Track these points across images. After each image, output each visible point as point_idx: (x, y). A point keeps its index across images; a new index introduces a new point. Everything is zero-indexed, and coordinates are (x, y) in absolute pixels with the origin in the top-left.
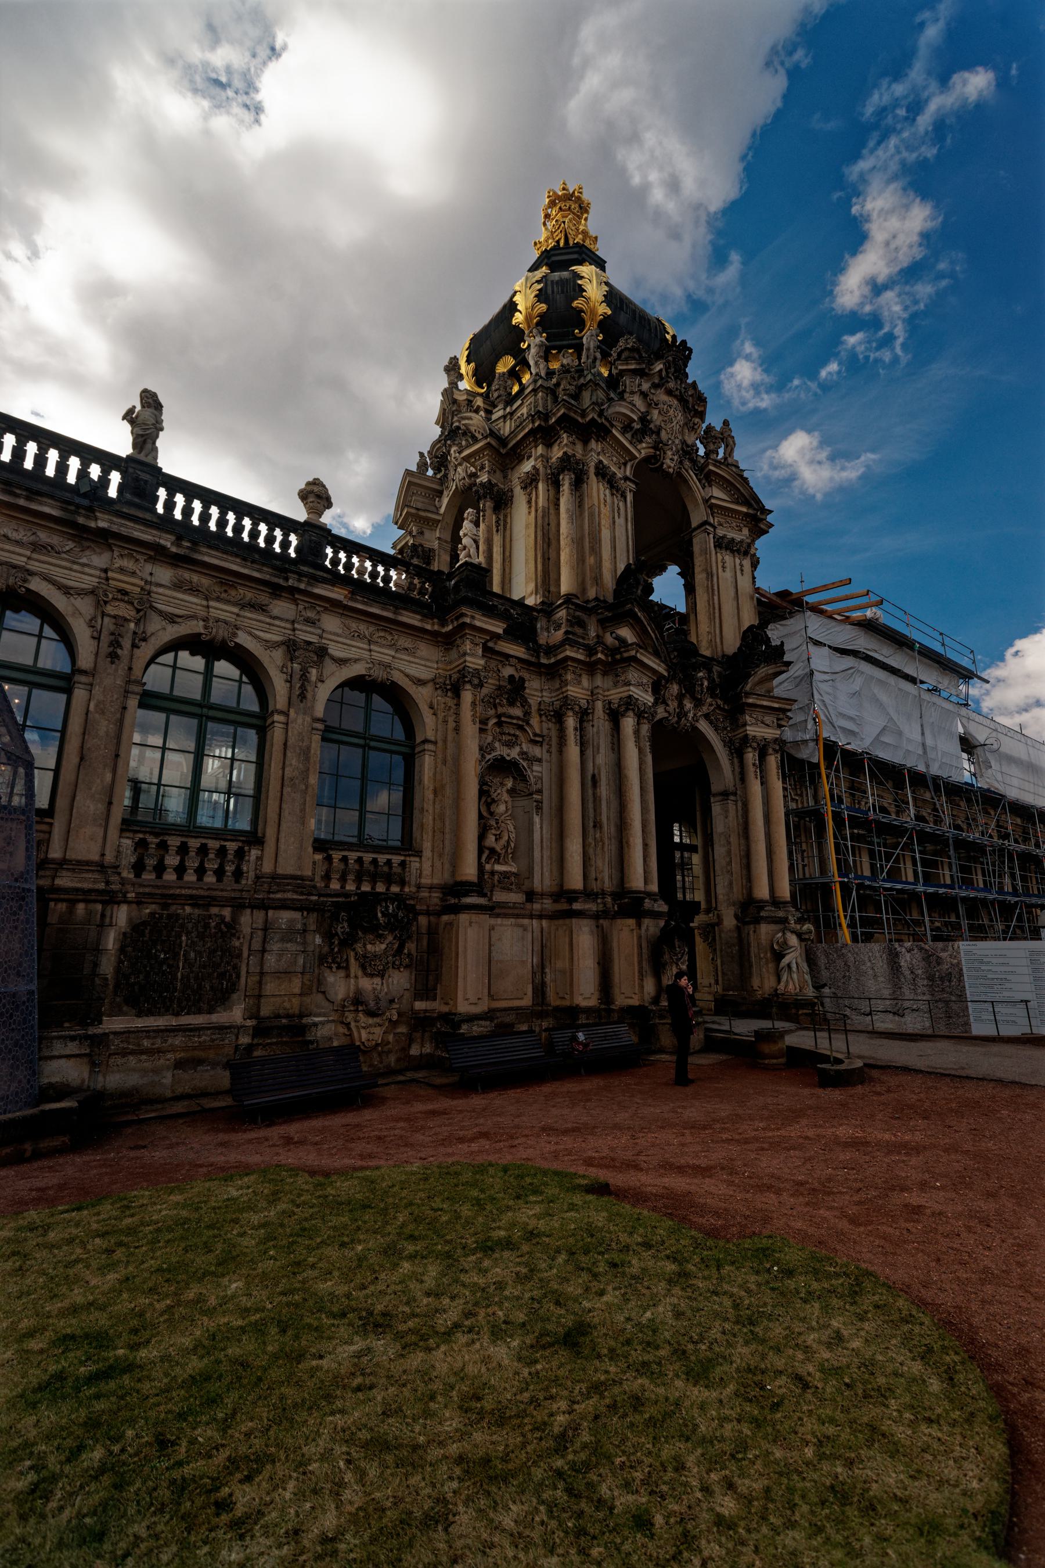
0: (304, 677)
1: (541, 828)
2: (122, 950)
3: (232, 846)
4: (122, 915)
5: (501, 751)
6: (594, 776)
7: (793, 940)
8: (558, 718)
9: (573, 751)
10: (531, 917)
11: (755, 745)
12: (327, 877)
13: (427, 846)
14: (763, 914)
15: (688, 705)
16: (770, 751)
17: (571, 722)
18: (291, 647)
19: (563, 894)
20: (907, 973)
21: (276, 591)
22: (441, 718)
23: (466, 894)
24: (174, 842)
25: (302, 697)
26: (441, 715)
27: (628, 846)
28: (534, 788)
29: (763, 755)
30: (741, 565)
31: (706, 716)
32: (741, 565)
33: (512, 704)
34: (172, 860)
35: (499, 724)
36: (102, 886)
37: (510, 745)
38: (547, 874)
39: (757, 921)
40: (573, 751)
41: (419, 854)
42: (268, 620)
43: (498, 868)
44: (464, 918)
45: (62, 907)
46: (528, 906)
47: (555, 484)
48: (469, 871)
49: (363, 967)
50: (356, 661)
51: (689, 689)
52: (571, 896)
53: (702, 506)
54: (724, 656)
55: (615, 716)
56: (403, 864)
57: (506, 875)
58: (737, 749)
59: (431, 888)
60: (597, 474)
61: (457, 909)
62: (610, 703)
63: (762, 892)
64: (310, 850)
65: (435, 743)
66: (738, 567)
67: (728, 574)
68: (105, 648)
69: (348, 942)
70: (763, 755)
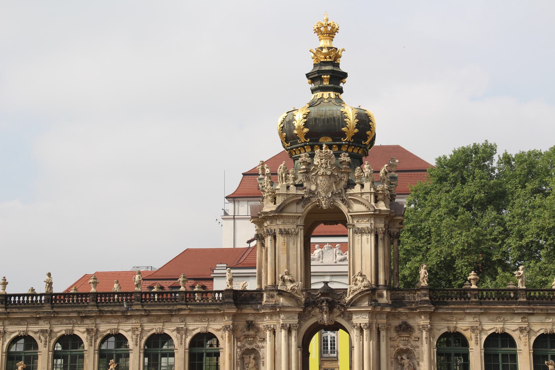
0: (182, 338)
5: (248, 346)
21: (172, 316)
25: (181, 344)
33: (249, 330)
37: (250, 344)
50: (197, 329)
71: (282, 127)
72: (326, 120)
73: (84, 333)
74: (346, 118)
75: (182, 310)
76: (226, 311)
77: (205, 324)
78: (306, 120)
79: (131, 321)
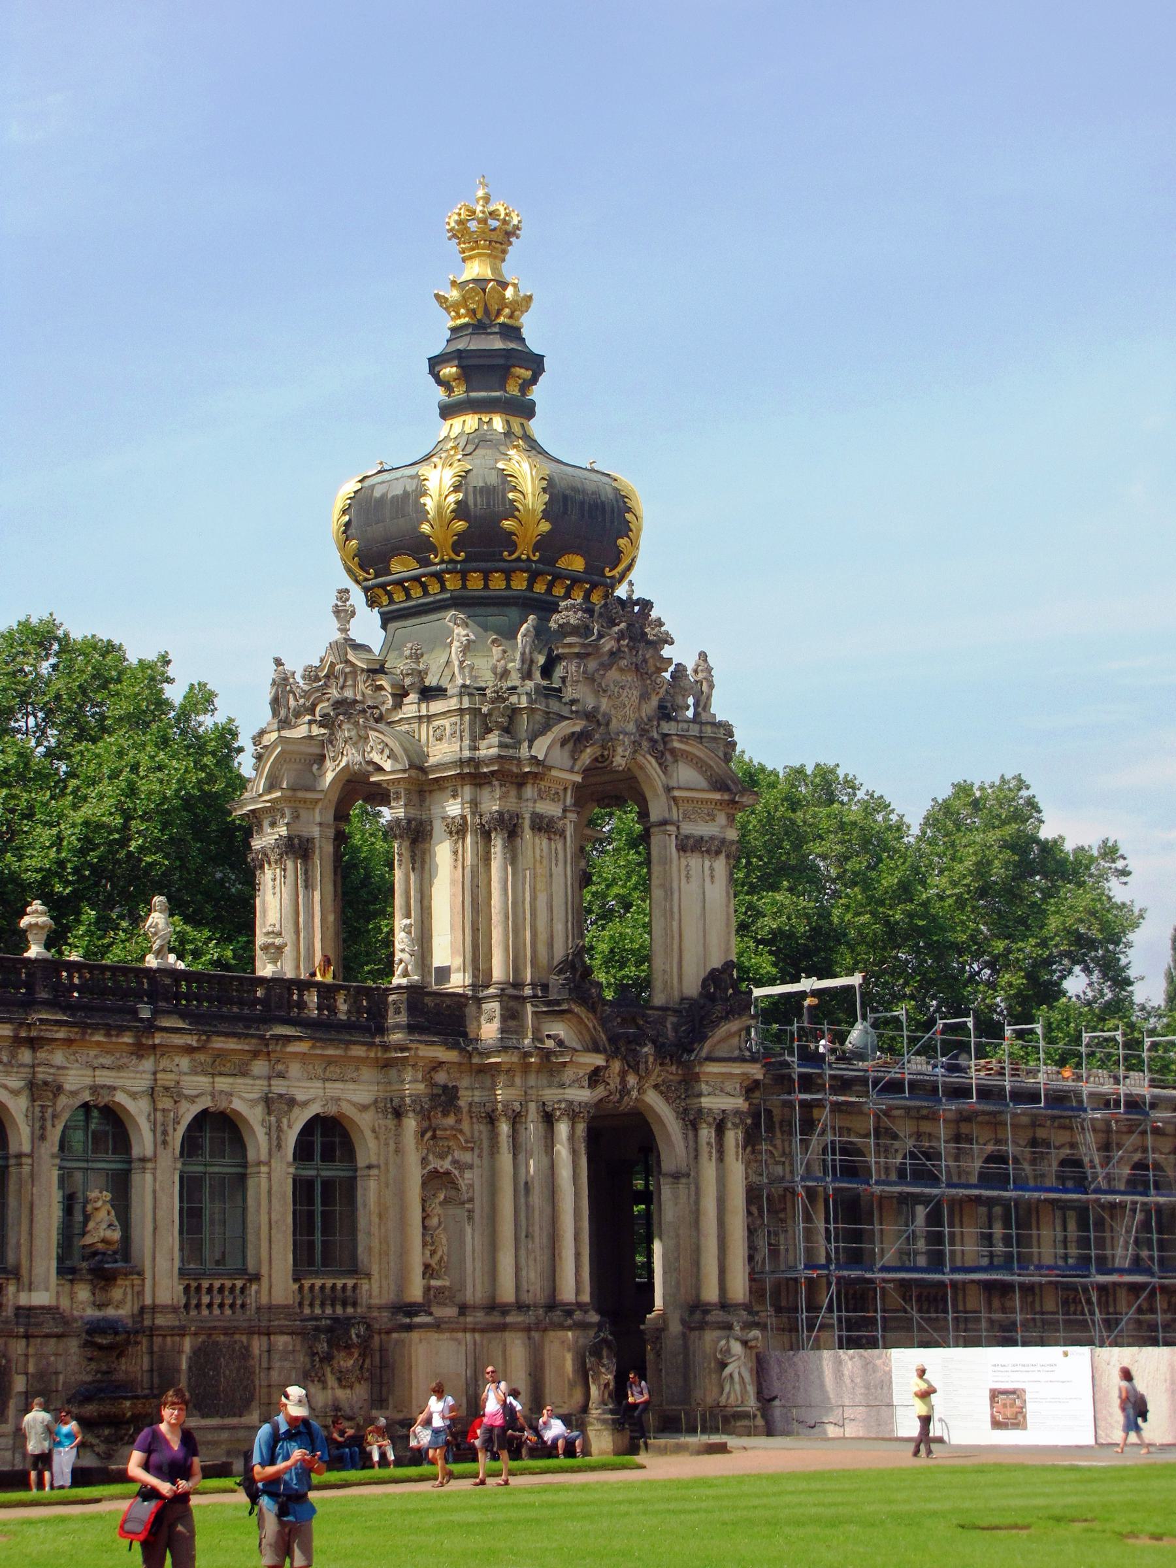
0: (279, 1129)
1: (473, 1239)
2: (190, 1368)
3: (239, 1284)
4: (187, 1344)
5: (436, 1164)
6: (526, 1183)
7: (737, 1348)
8: (491, 1120)
9: (505, 1158)
10: (465, 1330)
11: (710, 1120)
12: (301, 1304)
13: (375, 1270)
14: (709, 1318)
15: (632, 1080)
16: (729, 1125)
17: (504, 1128)
18: (268, 1101)
19: (493, 1306)
20: (848, 1381)
21: (255, 1054)
22: (382, 1142)
23: (416, 1314)
24: (205, 1284)
25: (279, 1146)
26: (382, 1138)
27: (560, 1258)
28: (465, 1197)
29: (720, 1129)
30: (712, 869)
31: (656, 1087)
32: (712, 869)
33: (445, 1114)
34: (206, 1299)
35: (434, 1137)
36: (177, 1323)
37: (442, 1157)
38: (479, 1287)
39: (702, 1326)
40: (505, 1158)
41: (368, 1276)
42: (251, 1082)
43: (433, 1283)
44: (415, 1335)
45: (160, 1339)
46: (462, 1319)
47: (486, 835)
48: (416, 1293)
49: (339, 1380)
50: (313, 1100)
51: (633, 1064)
52: (504, 1309)
53: (663, 798)
54: (682, 999)
55: (549, 1119)
56: (355, 1287)
57: (440, 1290)
58: (692, 1120)
59: (380, 1308)
60: (532, 828)
61: (409, 1328)
62: (544, 1104)
63: (711, 1294)
64: (291, 1281)
65: (378, 1167)
66: (707, 872)
67: (694, 885)
68: (159, 1138)
69: (328, 1358)
70: (720, 1129)
71: (458, 503)
72: (587, 508)
73: (15, 1093)
74: (629, 510)
75: (288, 1039)
76: (421, 1053)
77: (335, 1089)
78: (546, 497)
79: (148, 1064)
